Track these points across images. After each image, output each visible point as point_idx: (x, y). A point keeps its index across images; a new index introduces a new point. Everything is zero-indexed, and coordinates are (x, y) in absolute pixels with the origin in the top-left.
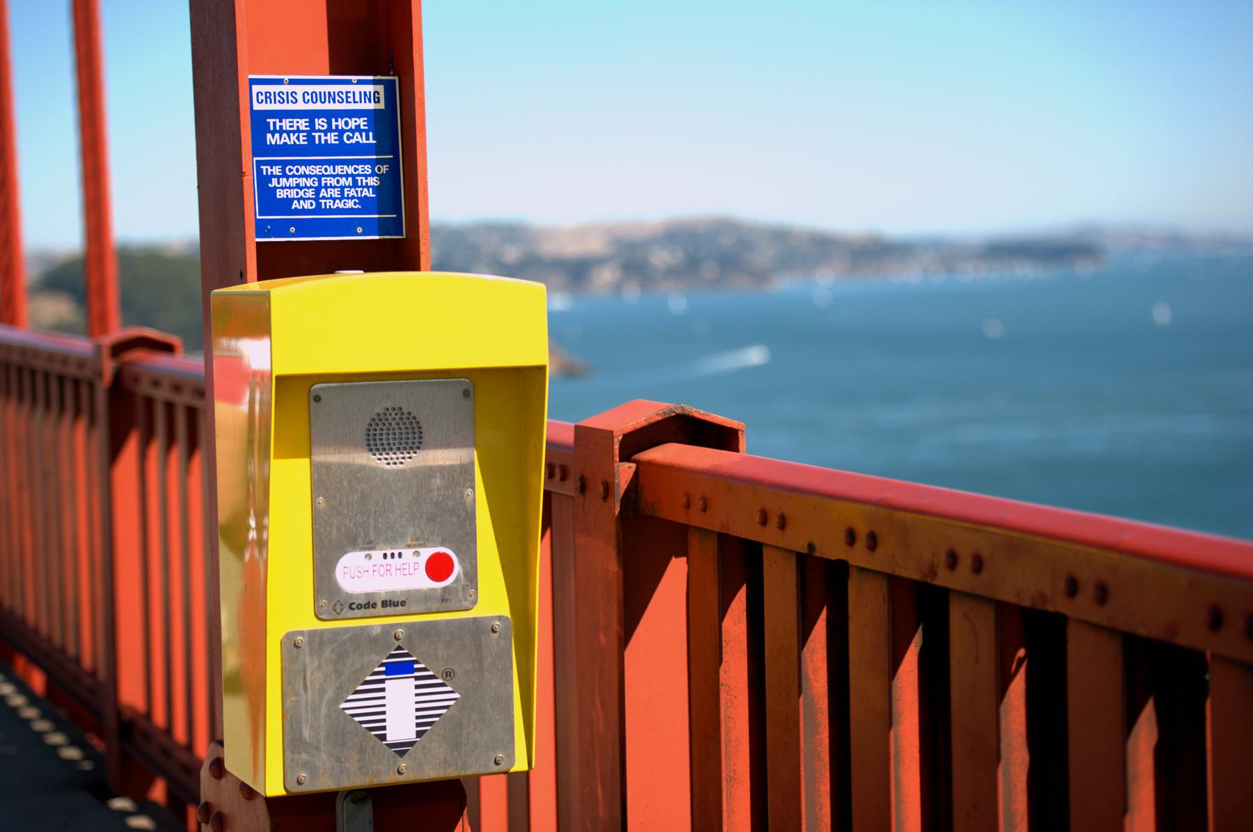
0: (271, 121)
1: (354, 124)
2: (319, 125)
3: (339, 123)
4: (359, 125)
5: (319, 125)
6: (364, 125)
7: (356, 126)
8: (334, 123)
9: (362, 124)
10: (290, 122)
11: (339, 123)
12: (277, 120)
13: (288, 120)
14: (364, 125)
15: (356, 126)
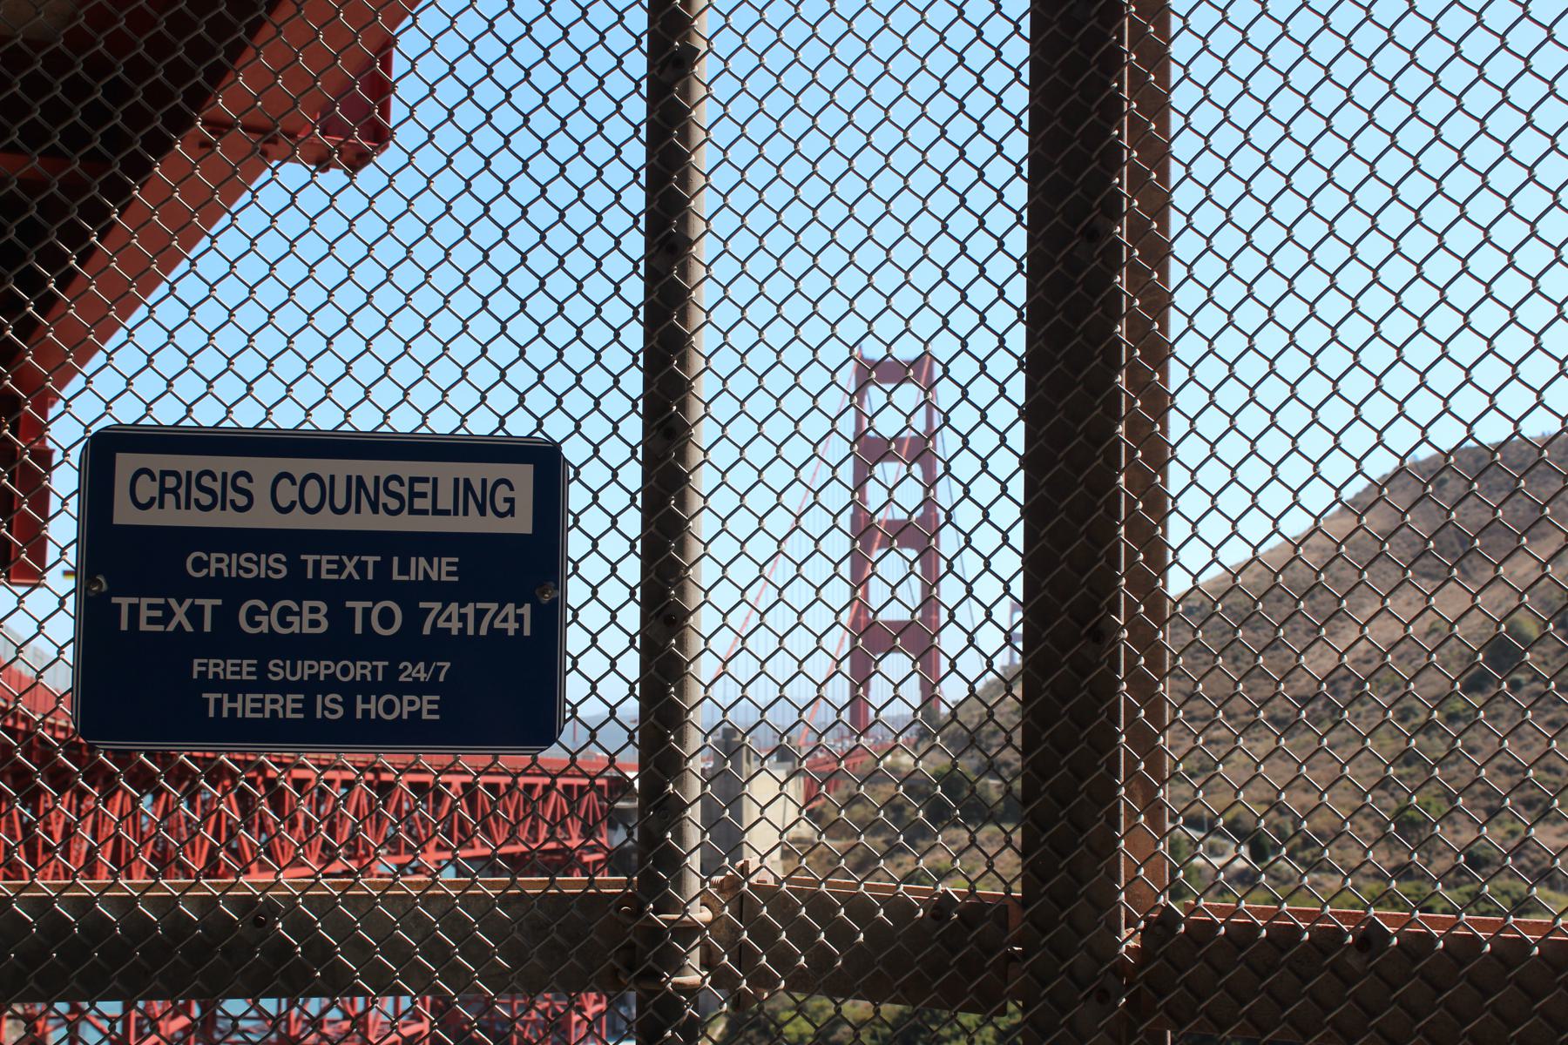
0: (212, 697)
1: (406, 709)
2: (324, 708)
3: (372, 706)
4: (421, 709)
5: (324, 708)
6: (430, 712)
7: (409, 712)
8: (360, 706)
9: (426, 707)
10: (253, 701)
11: (372, 706)
12: (226, 696)
13: (249, 697)
14: (430, 712)
15: (409, 712)
